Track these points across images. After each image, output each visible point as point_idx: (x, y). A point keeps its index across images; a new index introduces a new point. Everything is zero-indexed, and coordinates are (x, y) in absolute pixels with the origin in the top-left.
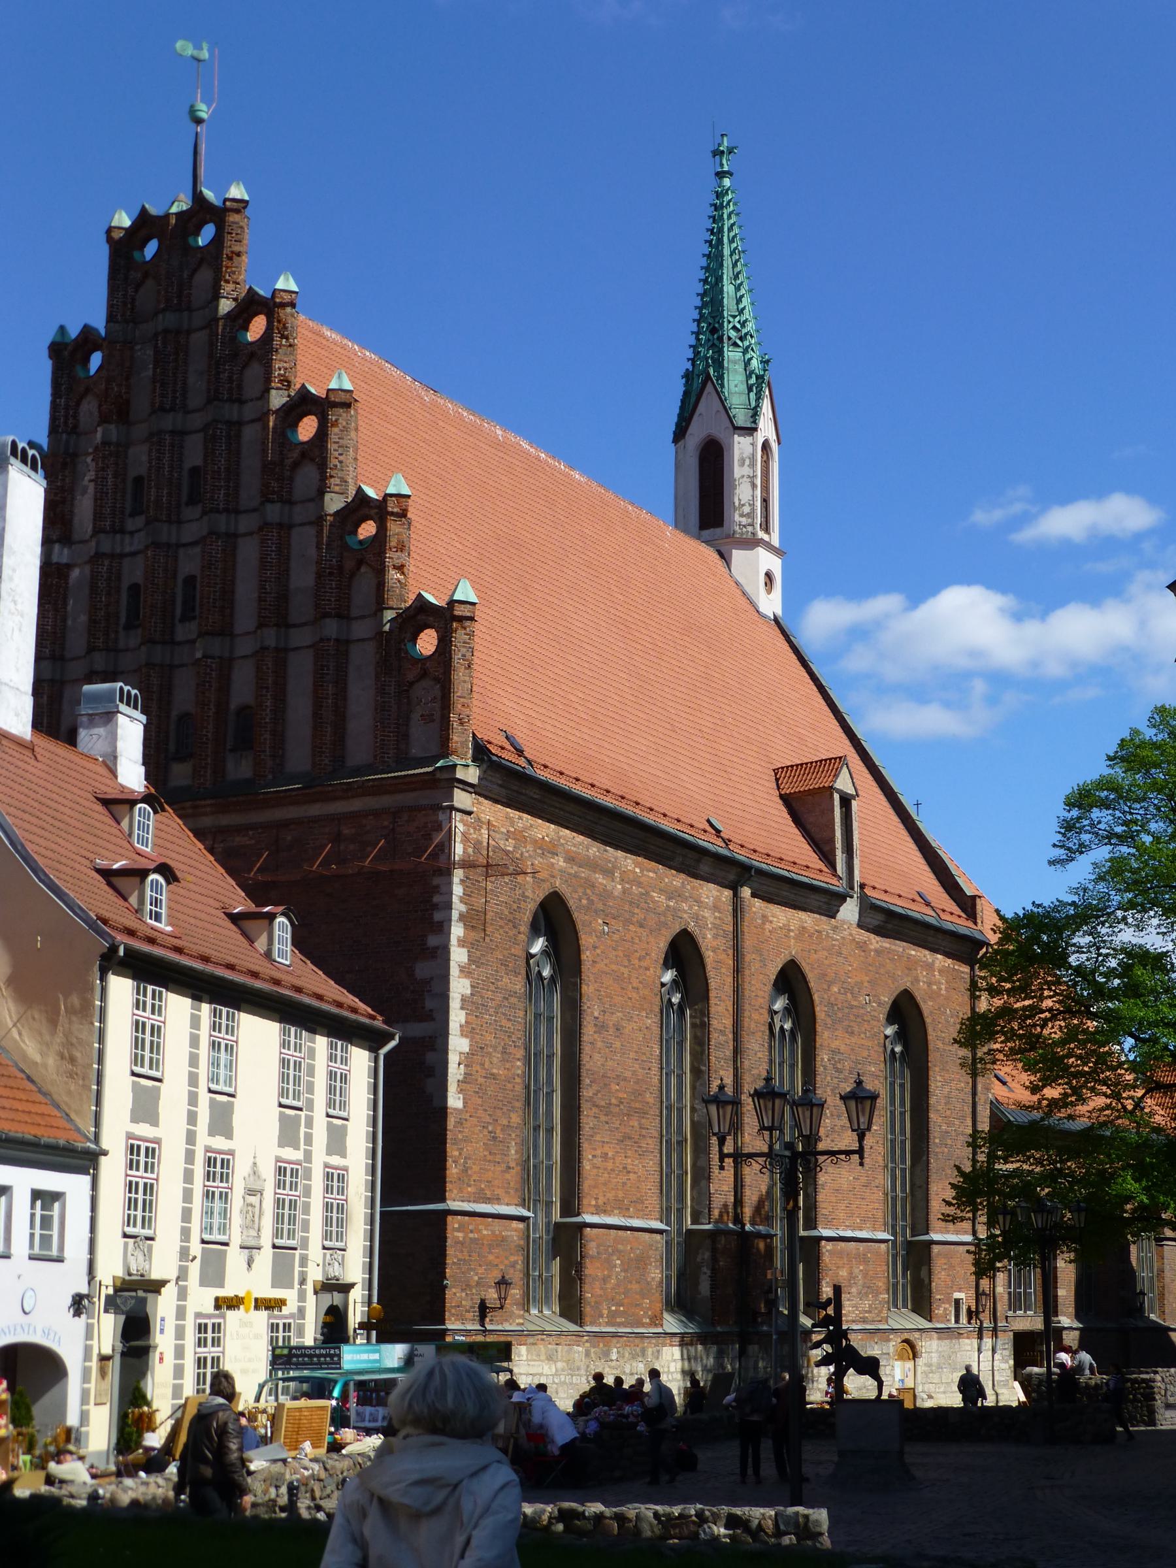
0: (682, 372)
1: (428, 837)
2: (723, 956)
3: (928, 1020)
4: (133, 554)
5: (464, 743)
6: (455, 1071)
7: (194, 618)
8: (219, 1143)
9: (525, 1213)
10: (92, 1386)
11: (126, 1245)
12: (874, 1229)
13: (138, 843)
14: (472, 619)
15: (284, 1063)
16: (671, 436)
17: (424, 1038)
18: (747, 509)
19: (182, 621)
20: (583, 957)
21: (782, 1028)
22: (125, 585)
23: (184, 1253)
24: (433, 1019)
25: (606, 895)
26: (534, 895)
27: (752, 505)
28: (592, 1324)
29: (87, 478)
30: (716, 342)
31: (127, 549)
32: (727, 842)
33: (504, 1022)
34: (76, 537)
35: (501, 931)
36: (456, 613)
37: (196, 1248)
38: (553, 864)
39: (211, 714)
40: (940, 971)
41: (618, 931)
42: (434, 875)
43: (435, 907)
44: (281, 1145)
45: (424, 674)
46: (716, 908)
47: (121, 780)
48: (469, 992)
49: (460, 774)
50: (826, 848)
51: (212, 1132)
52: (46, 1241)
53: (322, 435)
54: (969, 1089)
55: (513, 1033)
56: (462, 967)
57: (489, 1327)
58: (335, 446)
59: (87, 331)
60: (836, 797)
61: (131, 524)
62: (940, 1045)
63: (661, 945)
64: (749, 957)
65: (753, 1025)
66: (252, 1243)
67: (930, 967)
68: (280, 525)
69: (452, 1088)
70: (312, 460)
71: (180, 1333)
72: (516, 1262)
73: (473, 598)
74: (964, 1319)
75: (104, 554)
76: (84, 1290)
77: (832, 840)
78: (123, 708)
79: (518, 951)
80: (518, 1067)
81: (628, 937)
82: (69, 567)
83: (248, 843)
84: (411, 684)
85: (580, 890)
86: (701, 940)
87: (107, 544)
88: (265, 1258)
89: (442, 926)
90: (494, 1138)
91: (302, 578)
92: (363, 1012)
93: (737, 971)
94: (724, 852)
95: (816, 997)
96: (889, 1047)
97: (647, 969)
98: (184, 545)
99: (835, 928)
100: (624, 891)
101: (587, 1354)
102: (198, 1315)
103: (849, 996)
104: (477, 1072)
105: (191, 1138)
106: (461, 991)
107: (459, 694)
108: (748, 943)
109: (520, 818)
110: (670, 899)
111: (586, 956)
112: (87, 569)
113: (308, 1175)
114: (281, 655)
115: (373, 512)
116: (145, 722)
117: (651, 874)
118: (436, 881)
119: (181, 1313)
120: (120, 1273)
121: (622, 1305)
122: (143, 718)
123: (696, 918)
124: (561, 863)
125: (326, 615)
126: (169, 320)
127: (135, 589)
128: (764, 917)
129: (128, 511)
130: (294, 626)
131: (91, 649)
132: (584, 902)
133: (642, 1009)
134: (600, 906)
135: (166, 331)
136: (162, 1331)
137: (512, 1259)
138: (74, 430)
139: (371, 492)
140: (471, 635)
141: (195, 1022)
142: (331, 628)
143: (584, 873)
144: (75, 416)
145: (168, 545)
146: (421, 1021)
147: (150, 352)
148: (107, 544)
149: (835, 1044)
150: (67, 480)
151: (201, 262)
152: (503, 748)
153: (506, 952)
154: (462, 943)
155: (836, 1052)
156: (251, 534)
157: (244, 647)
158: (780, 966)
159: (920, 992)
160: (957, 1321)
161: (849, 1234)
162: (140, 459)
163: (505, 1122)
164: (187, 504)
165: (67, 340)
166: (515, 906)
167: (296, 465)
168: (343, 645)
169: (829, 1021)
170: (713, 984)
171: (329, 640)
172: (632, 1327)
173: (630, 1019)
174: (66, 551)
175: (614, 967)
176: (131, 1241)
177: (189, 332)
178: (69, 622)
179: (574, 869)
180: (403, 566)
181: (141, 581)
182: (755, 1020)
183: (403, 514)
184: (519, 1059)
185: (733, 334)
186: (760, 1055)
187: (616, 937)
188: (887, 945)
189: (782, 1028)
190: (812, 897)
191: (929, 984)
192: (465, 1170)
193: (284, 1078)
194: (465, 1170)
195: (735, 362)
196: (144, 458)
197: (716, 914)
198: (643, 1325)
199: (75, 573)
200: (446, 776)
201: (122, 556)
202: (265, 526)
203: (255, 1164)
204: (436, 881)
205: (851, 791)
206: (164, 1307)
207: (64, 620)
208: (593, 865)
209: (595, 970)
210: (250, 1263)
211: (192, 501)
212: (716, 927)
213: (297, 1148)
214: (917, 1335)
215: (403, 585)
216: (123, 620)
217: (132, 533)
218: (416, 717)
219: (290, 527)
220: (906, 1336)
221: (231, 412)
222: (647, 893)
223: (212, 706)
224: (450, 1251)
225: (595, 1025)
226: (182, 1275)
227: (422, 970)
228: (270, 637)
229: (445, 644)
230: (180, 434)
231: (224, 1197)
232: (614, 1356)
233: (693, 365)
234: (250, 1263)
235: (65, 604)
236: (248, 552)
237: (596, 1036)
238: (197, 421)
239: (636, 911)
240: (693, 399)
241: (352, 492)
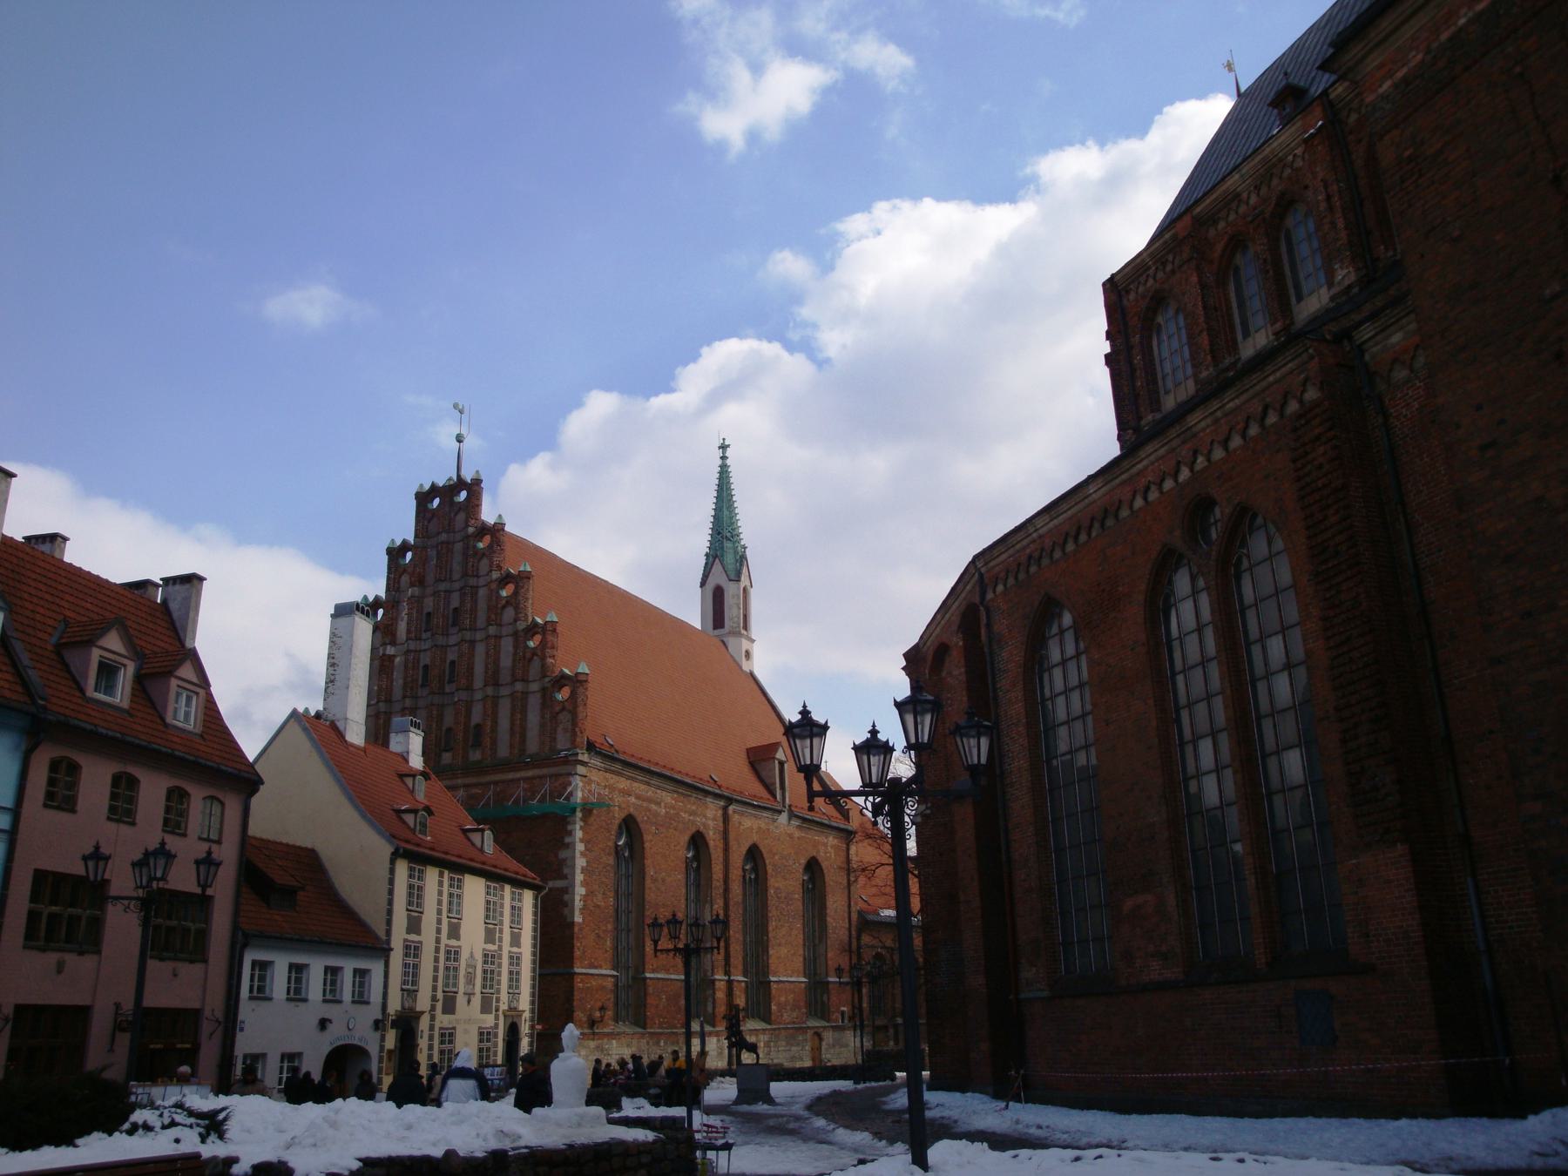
0: (705, 553)
1: (565, 789)
3: (825, 871)
4: (425, 650)
5: (583, 743)
6: (578, 904)
7: (454, 681)
8: (453, 942)
9: (615, 973)
10: (384, 1065)
11: (403, 995)
12: (798, 976)
14: (586, 681)
15: (488, 902)
16: (699, 584)
18: (736, 619)
19: (449, 683)
21: (750, 877)
22: (422, 664)
23: (434, 999)
25: (656, 815)
26: (619, 816)
27: (739, 618)
28: (651, 1028)
29: (404, 613)
31: (423, 648)
32: (720, 787)
33: (604, 880)
34: (398, 642)
36: (579, 679)
37: (440, 995)
40: (831, 847)
44: (485, 943)
45: (563, 709)
46: (714, 819)
47: (410, 764)
48: (585, 864)
49: (580, 757)
50: (771, 788)
51: (449, 937)
52: (361, 994)
53: (516, 593)
54: (847, 904)
57: (597, 1031)
59: (405, 543)
60: (776, 762)
61: (424, 636)
62: (832, 883)
63: (686, 838)
64: (732, 843)
66: (470, 991)
67: (825, 845)
68: (496, 636)
69: (577, 913)
70: (511, 605)
71: (431, 1038)
72: (609, 999)
73: (587, 671)
74: (846, 1021)
75: (411, 651)
76: (380, 1017)
77: (775, 783)
78: (412, 729)
79: (611, 844)
82: (394, 656)
84: (557, 713)
87: (412, 645)
88: (477, 1001)
90: (599, 936)
91: (506, 661)
92: (530, 875)
93: (726, 849)
94: (717, 791)
95: (767, 862)
96: (805, 885)
98: (450, 646)
99: (776, 827)
100: (667, 812)
101: (648, 1043)
102: (441, 1028)
103: (784, 861)
105: (438, 941)
108: (732, 835)
109: (612, 778)
111: (647, 845)
112: (403, 658)
113: (500, 957)
114: (496, 699)
115: (540, 630)
117: (681, 804)
119: (432, 1028)
120: (399, 1009)
121: (666, 1018)
122: (423, 734)
123: (704, 825)
125: (516, 680)
126: (444, 537)
127: (426, 667)
128: (740, 823)
129: (423, 629)
130: (502, 685)
131: (404, 697)
132: (645, 818)
134: (654, 820)
135: (442, 543)
136: (421, 1037)
137: (608, 996)
138: (398, 590)
139: (539, 621)
140: (586, 689)
141: (441, 884)
142: (519, 686)
143: (645, 804)
144: (399, 582)
145: (442, 646)
147: (435, 553)
148: (412, 645)
149: (777, 885)
150: (395, 614)
151: (460, 509)
152: (602, 744)
155: (778, 888)
156: (482, 641)
157: (478, 696)
159: (821, 856)
160: (842, 1022)
161: (785, 979)
162: (429, 604)
163: (604, 928)
164: (452, 626)
165: (395, 546)
167: (504, 607)
168: (525, 694)
169: (773, 873)
170: (713, 857)
171: (518, 692)
172: (671, 1029)
174: (393, 648)
176: (405, 993)
177: (454, 543)
178: (395, 683)
180: (554, 656)
181: (429, 663)
182: (736, 874)
183: (554, 630)
185: (728, 535)
187: (662, 835)
188: (803, 835)
189: (750, 877)
191: (826, 853)
192: (584, 952)
193: (488, 910)
194: (584, 952)
195: (730, 548)
196: (431, 604)
198: (676, 1028)
199: (398, 660)
200: (574, 758)
201: (420, 651)
202: (488, 637)
203: (472, 952)
205: (784, 759)
206: (424, 1023)
207: (392, 682)
208: (650, 800)
210: (469, 1002)
211: (454, 624)
213: (494, 944)
214: (822, 1030)
215: (554, 665)
216: (420, 682)
217: (425, 640)
218: (560, 729)
219: (501, 637)
220: (816, 1030)
221: (472, 581)
222: (678, 813)
224: (576, 993)
226: (433, 1008)
227: (563, 854)
228: (490, 691)
229: (573, 694)
230: (448, 592)
231: (456, 969)
232: (662, 1044)
234: (469, 1002)
235: (392, 674)
236: (480, 649)
238: (457, 585)
240: (709, 567)
241: (530, 619)
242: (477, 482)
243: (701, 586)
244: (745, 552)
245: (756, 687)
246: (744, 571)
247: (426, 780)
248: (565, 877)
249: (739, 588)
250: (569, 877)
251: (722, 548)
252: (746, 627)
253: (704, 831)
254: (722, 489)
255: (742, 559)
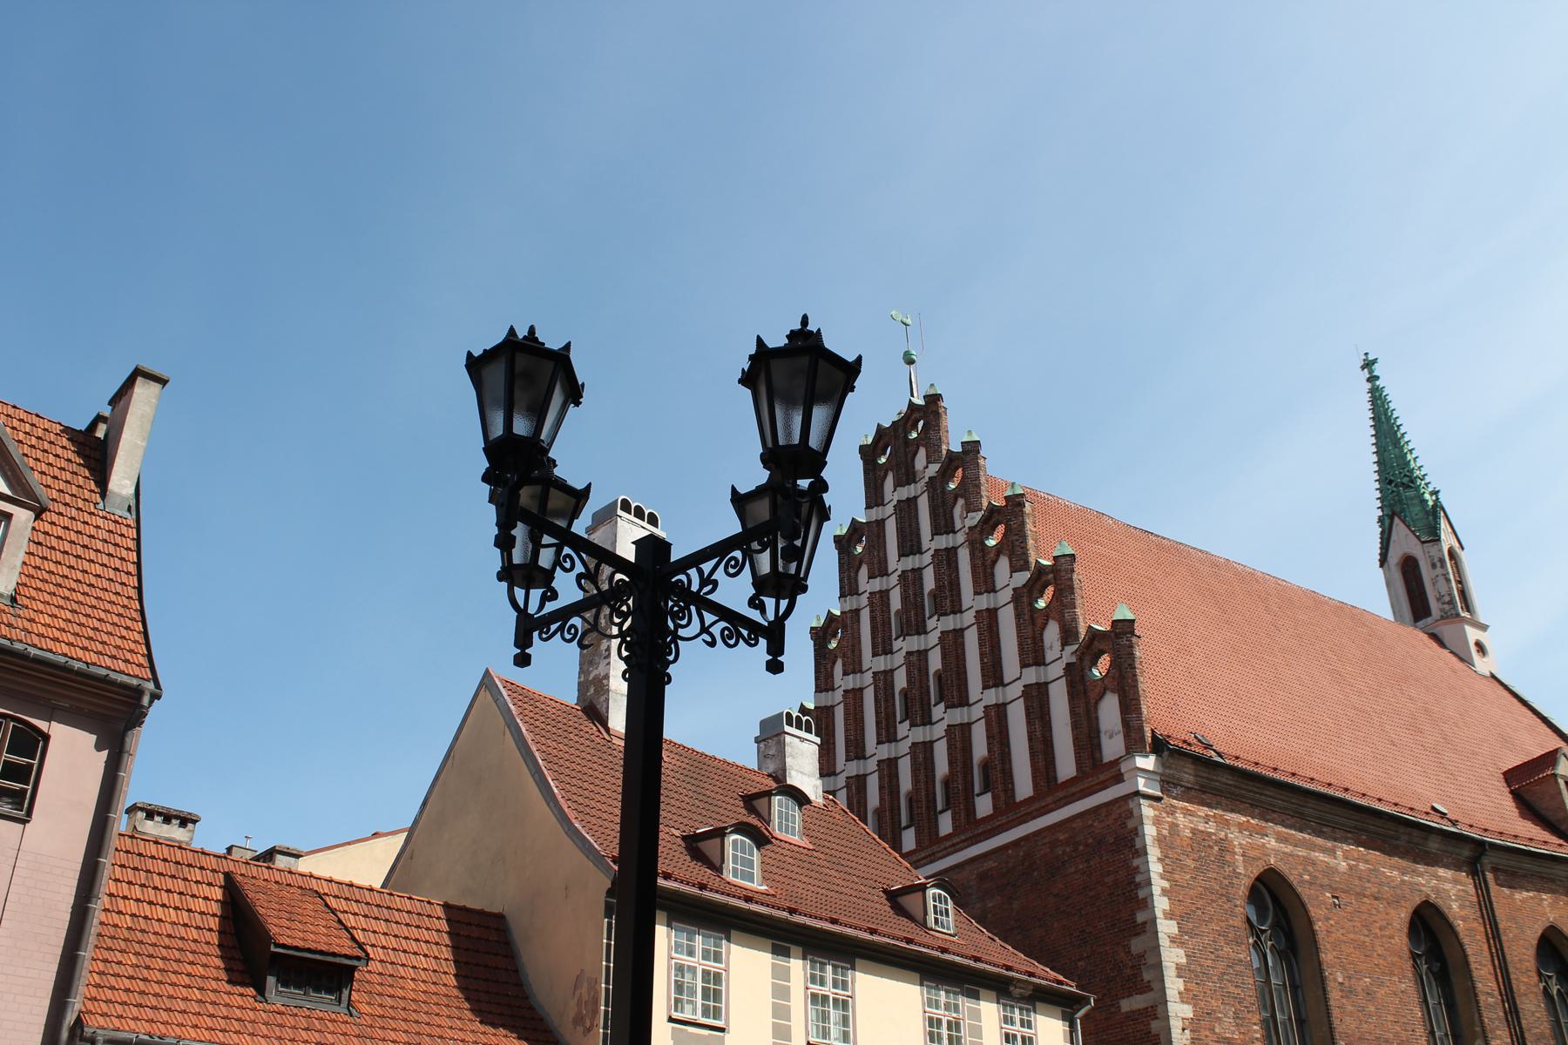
2: (1475, 925)
13: (780, 830)
15: (933, 1023)
17: (1147, 1008)
18: (1447, 599)
20: (1316, 928)
24: (1152, 989)
25: (1330, 871)
26: (1245, 874)
30: (1395, 489)
32: (1454, 823)
33: (1232, 989)
35: (1214, 905)
38: (1264, 844)
39: (959, 769)
41: (1351, 903)
42: (1133, 858)
43: (1138, 886)
48: (1184, 961)
55: (1245, 1000)
56: (1173, 937)
58: (1016, 537)
65: (1523, 988)
78: (787, 729)
80: (1255, 1031)
81: (1363, 908)
83: (993, 865)
85: (1300, 868)
86: (1446, 911)
89: (1147, 902)
93: (1494, 933)
97: (1392, 937)
100: (1351, 867)
104: (1206, 1036)
106: (1175, 960)
107: (1131, 697)
110: (1403, 874)
111: (1319, 926)
116: (819, 743)
118: (1136, 862)
122: (818, 740)
123: (1436, 890)
124: (1273, 842)
132: (1306, 877)
133: (1392, 974)
143: (1302, 852)
146: (1141, 993)
153: (1223, 924)
154: (1169, 915)
158: (1540, 932)
166: (1226, 882)
167: (994, 562)
173: (1382, 984)
175: (1352, 936)
179: (1289, 849)
184: (1255, 1024)
186: (1538, 1015)
187: (1349, 909)
190: (1558, 867)
197: (1459, 887)
204: (1136, 862)
209: (1331, 939)
212: (1458, 898)
223: (959, 764)
225: (1342, 991)
227: (1137, 945)
233: (1382, 511)
236: (972, 640)
237: (1344, 1001)
239: (1367, 885)
242: (933, 400)
243: (1381, 566)
244: (1438, 499)
245: (1505, 693)
246: (1443, 526)
247: (800, 806)
248: (1146, 988)
249: (1441, 550)
250: (1153, 985)
251: (1400, 501)
252: (1467, 606)
253: (1439, 902)
254: (1380, 419)
255: (1437, 510)
